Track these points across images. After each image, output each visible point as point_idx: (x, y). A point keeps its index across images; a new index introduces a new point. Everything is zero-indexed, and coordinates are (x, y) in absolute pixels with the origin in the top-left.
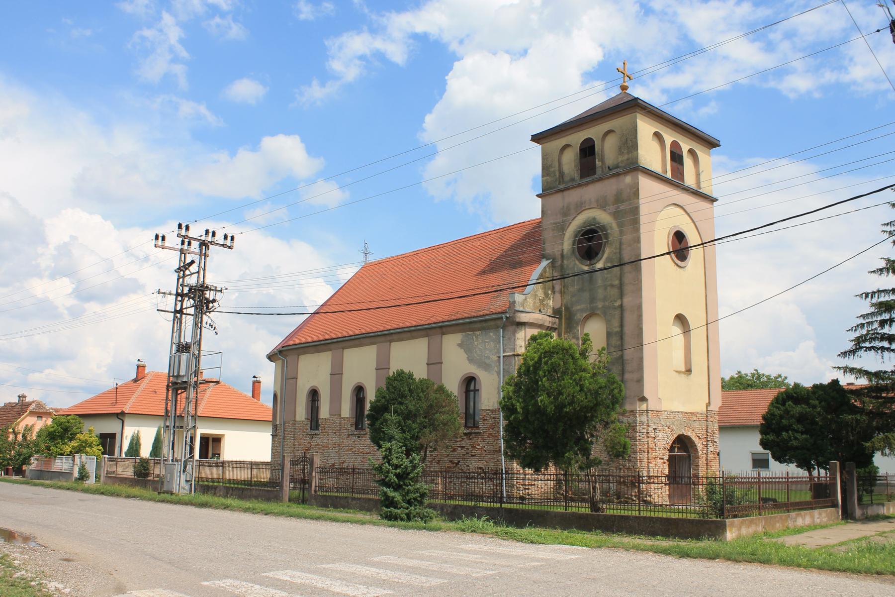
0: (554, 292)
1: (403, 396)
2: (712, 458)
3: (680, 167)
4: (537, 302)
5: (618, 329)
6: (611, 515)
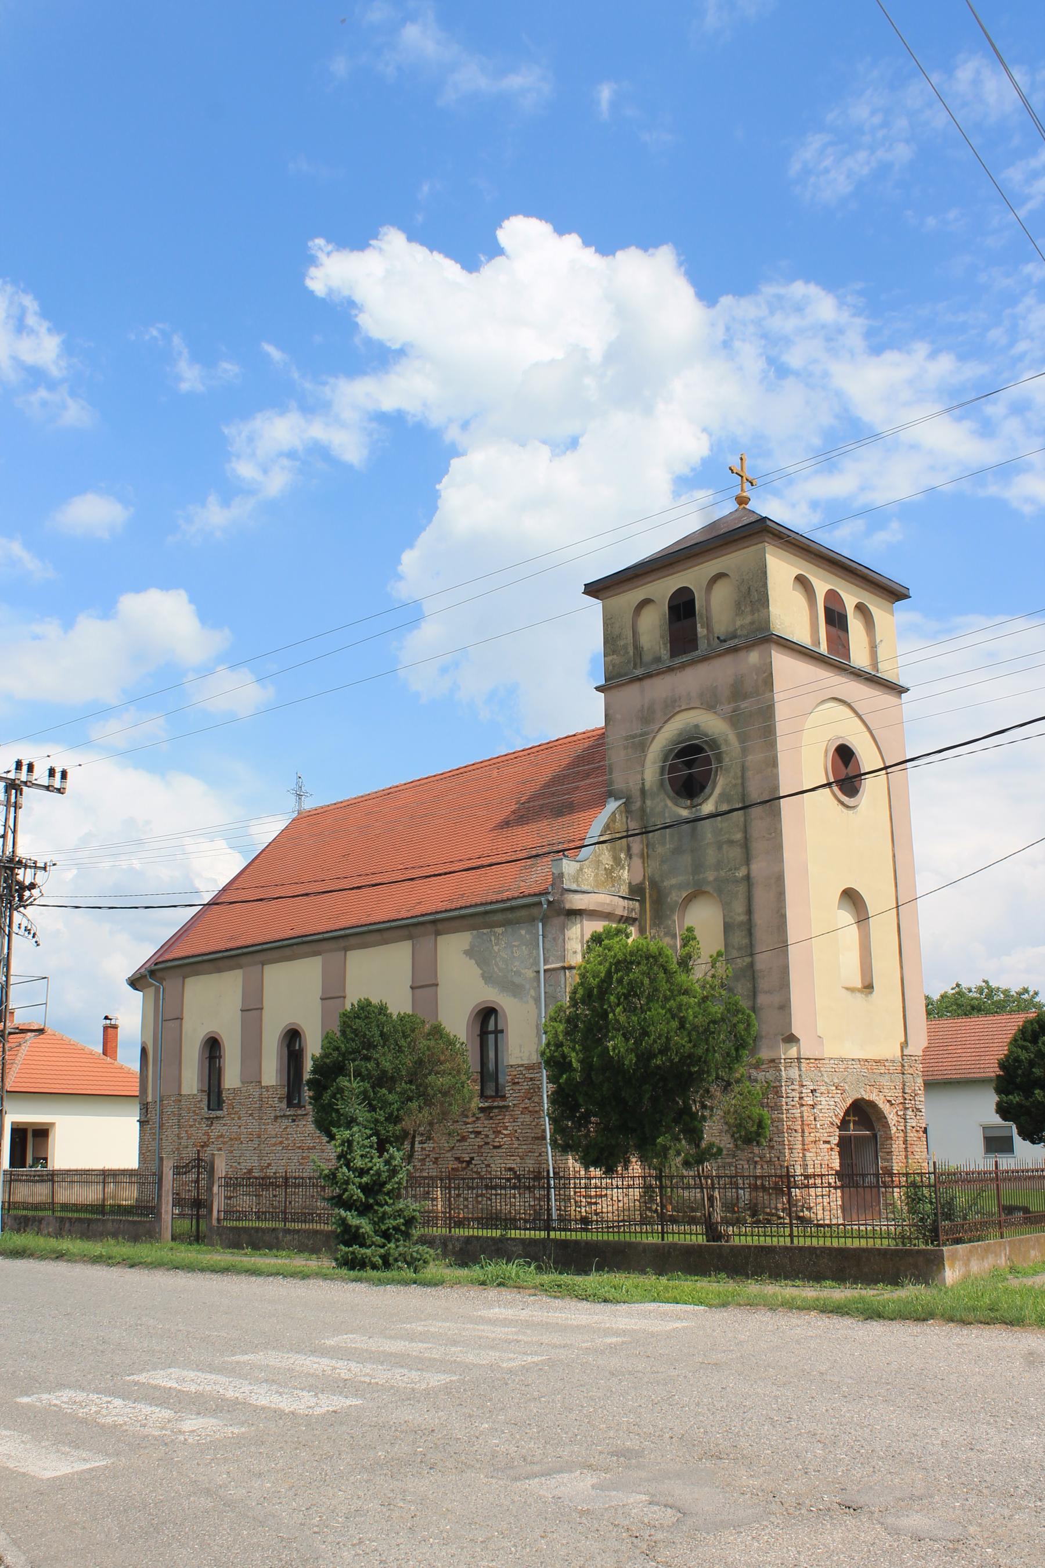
0: (630, 856)
1: (370, 1045)
2: (915, 1139)
3: (841, 634)
4: (602, 875)
5: (743, 918)
6: (743, 1246)
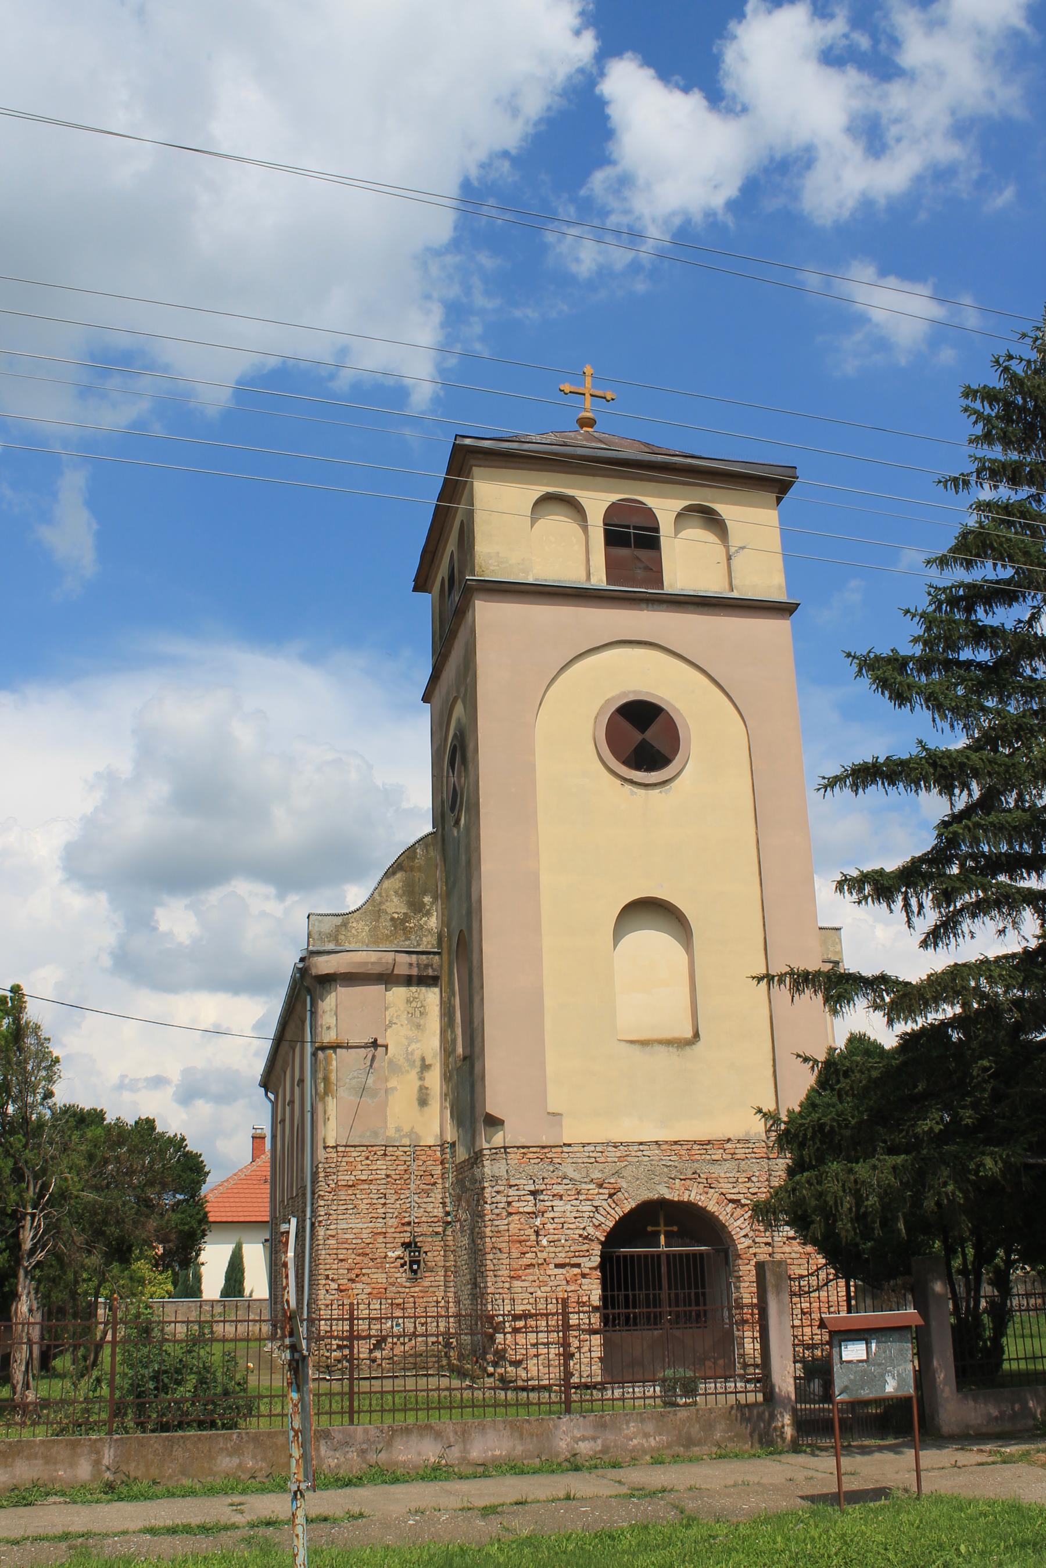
2: (794, 1255)
4: (385, 927)
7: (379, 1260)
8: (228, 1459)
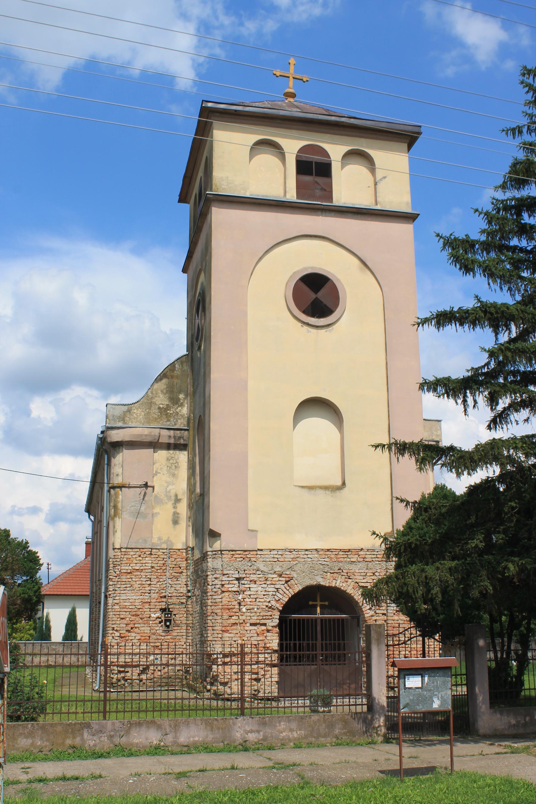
7: (145, 619)
8: (25, 740)
